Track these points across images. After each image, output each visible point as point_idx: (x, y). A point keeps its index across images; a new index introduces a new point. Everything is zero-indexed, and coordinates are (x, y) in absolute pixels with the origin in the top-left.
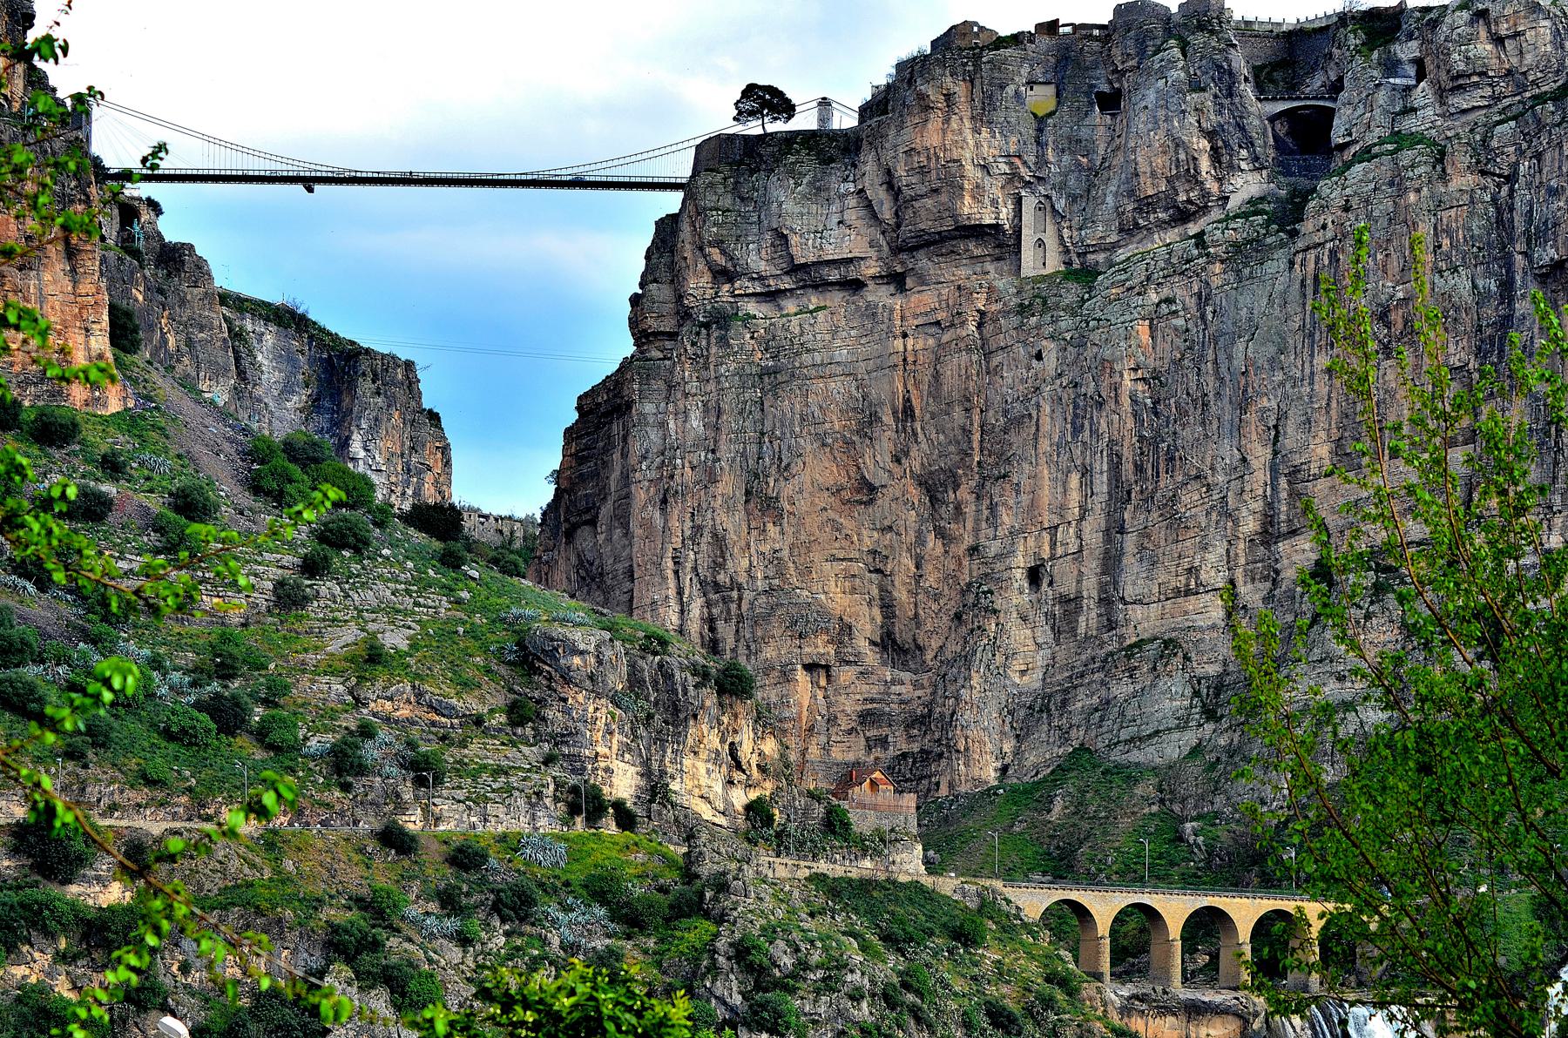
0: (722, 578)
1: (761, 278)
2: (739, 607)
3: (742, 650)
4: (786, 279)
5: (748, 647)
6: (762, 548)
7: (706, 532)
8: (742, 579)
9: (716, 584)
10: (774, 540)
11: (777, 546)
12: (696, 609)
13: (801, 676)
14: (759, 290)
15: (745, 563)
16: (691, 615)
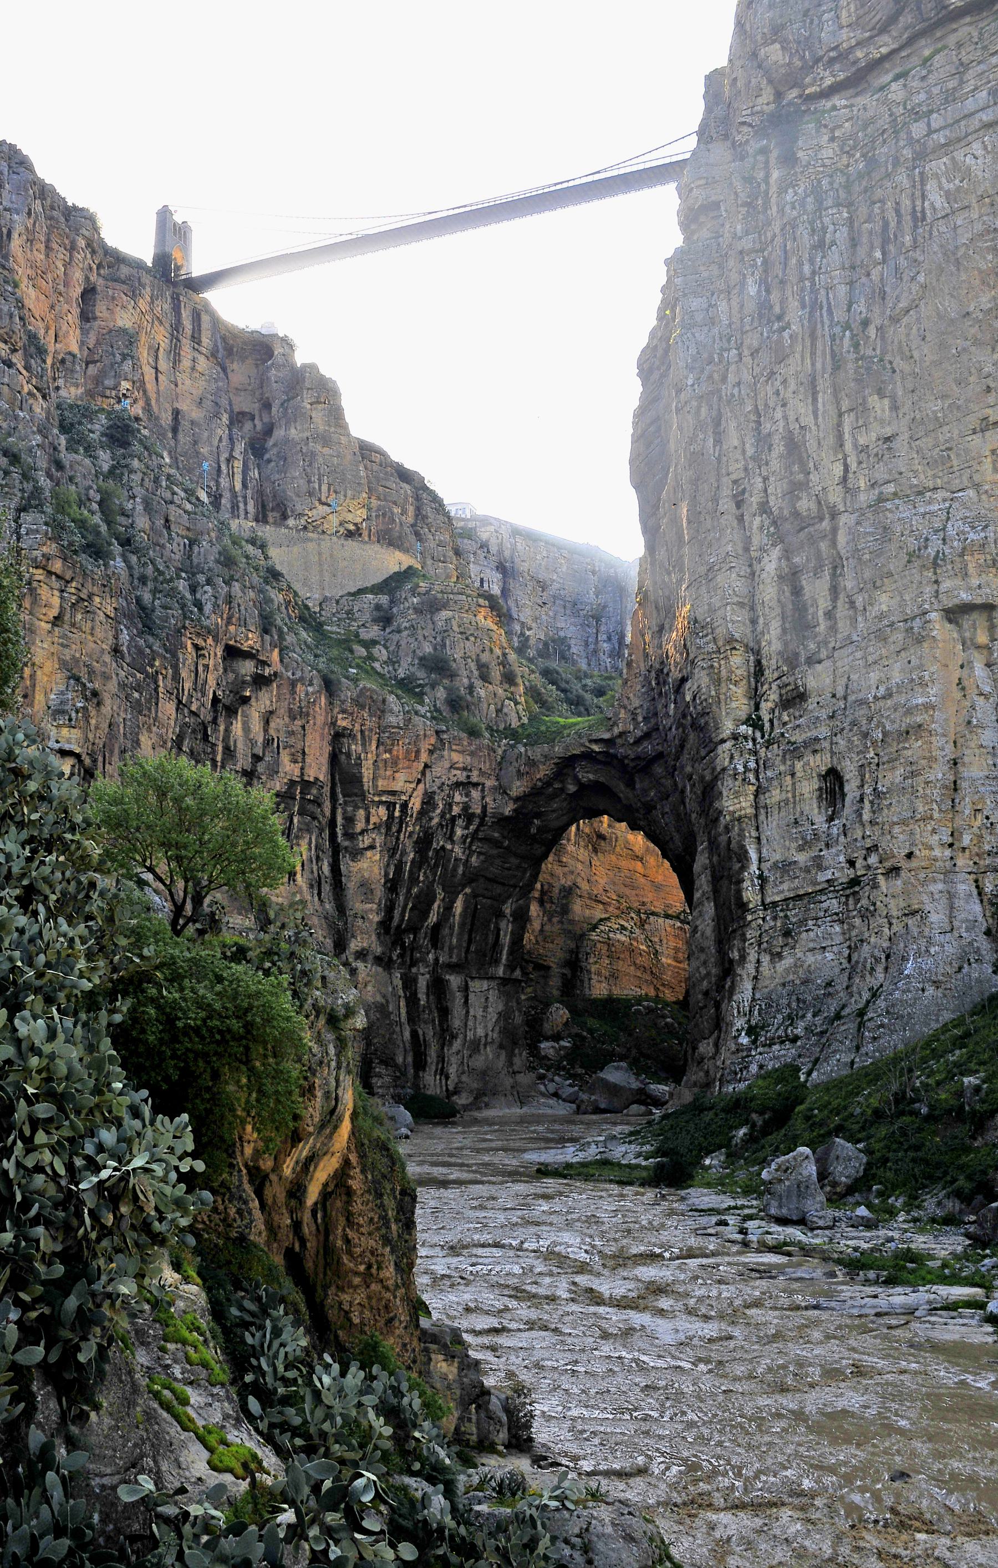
0: (805, 505)
1: (842, 56)
2: (834, 543)
3: (842, 611)
4: (885, 38)
5: (852, 604)
6: (862, 441)
7: (776, 439)
8: (835, 496)
9: (796, 514)
10: (882, 422)
11: (888, 431)
12: (771, 564)
13: (939, 628)
14: (842, 76)
15: (838, 470)
16: (764, 575)
